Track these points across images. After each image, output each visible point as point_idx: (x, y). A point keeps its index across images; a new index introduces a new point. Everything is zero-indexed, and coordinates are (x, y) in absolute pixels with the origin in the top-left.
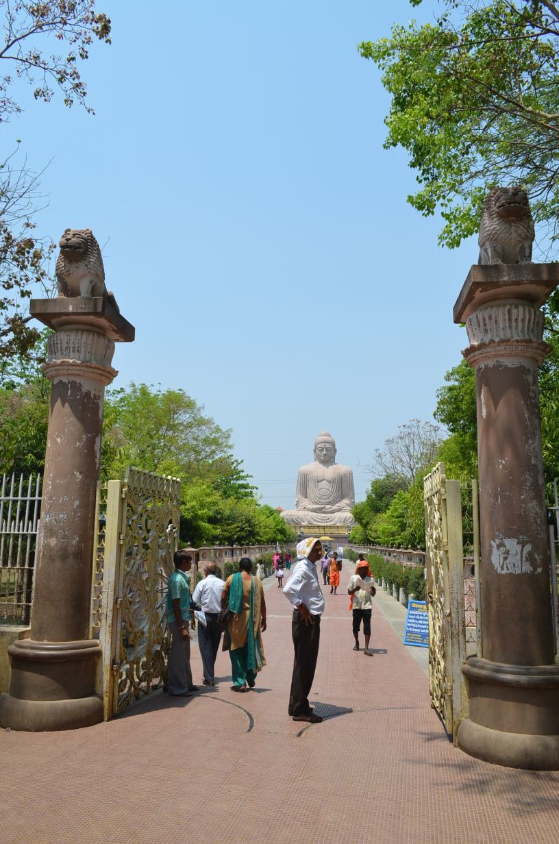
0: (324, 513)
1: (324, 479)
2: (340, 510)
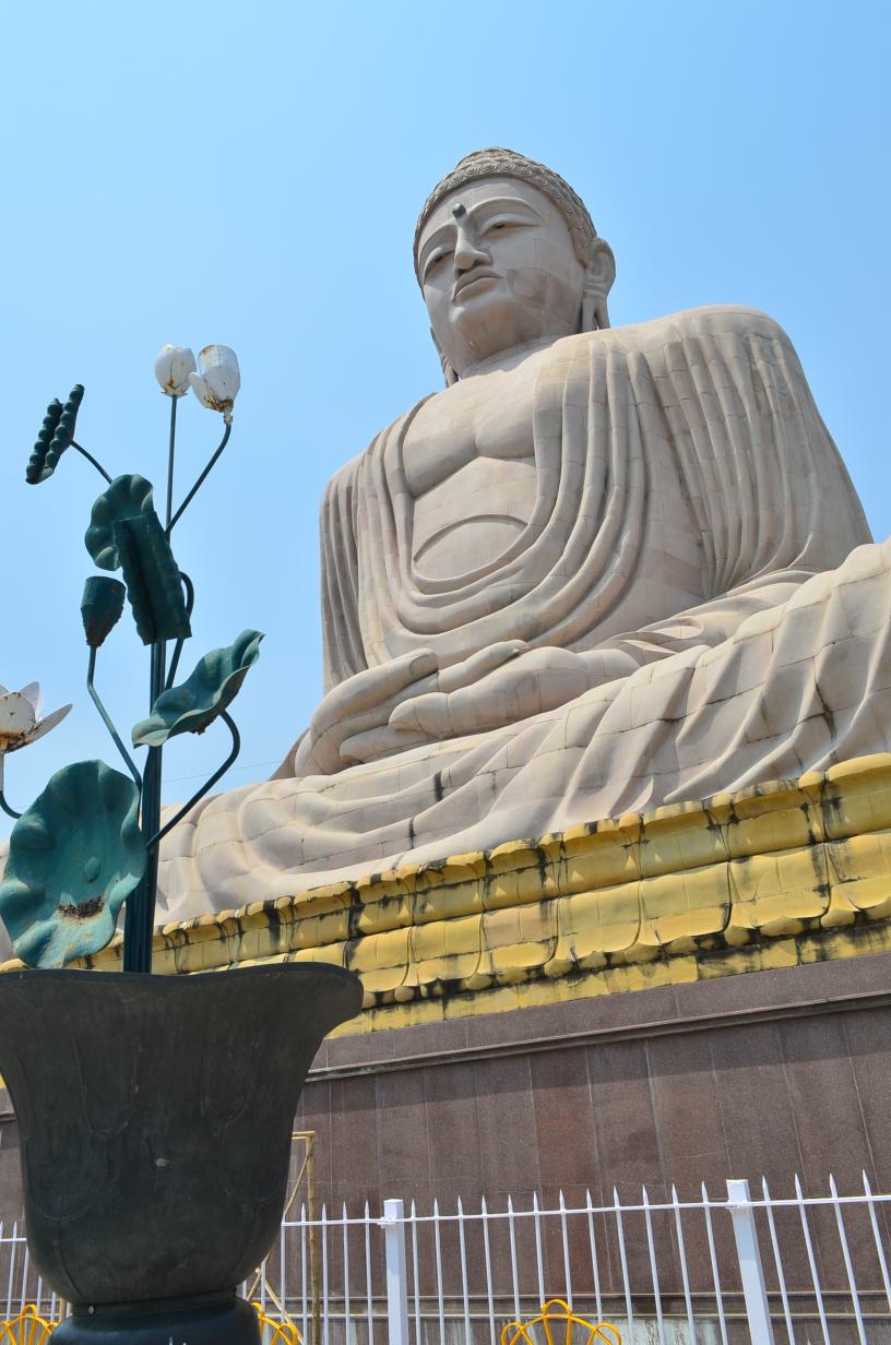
1: (472, 451)
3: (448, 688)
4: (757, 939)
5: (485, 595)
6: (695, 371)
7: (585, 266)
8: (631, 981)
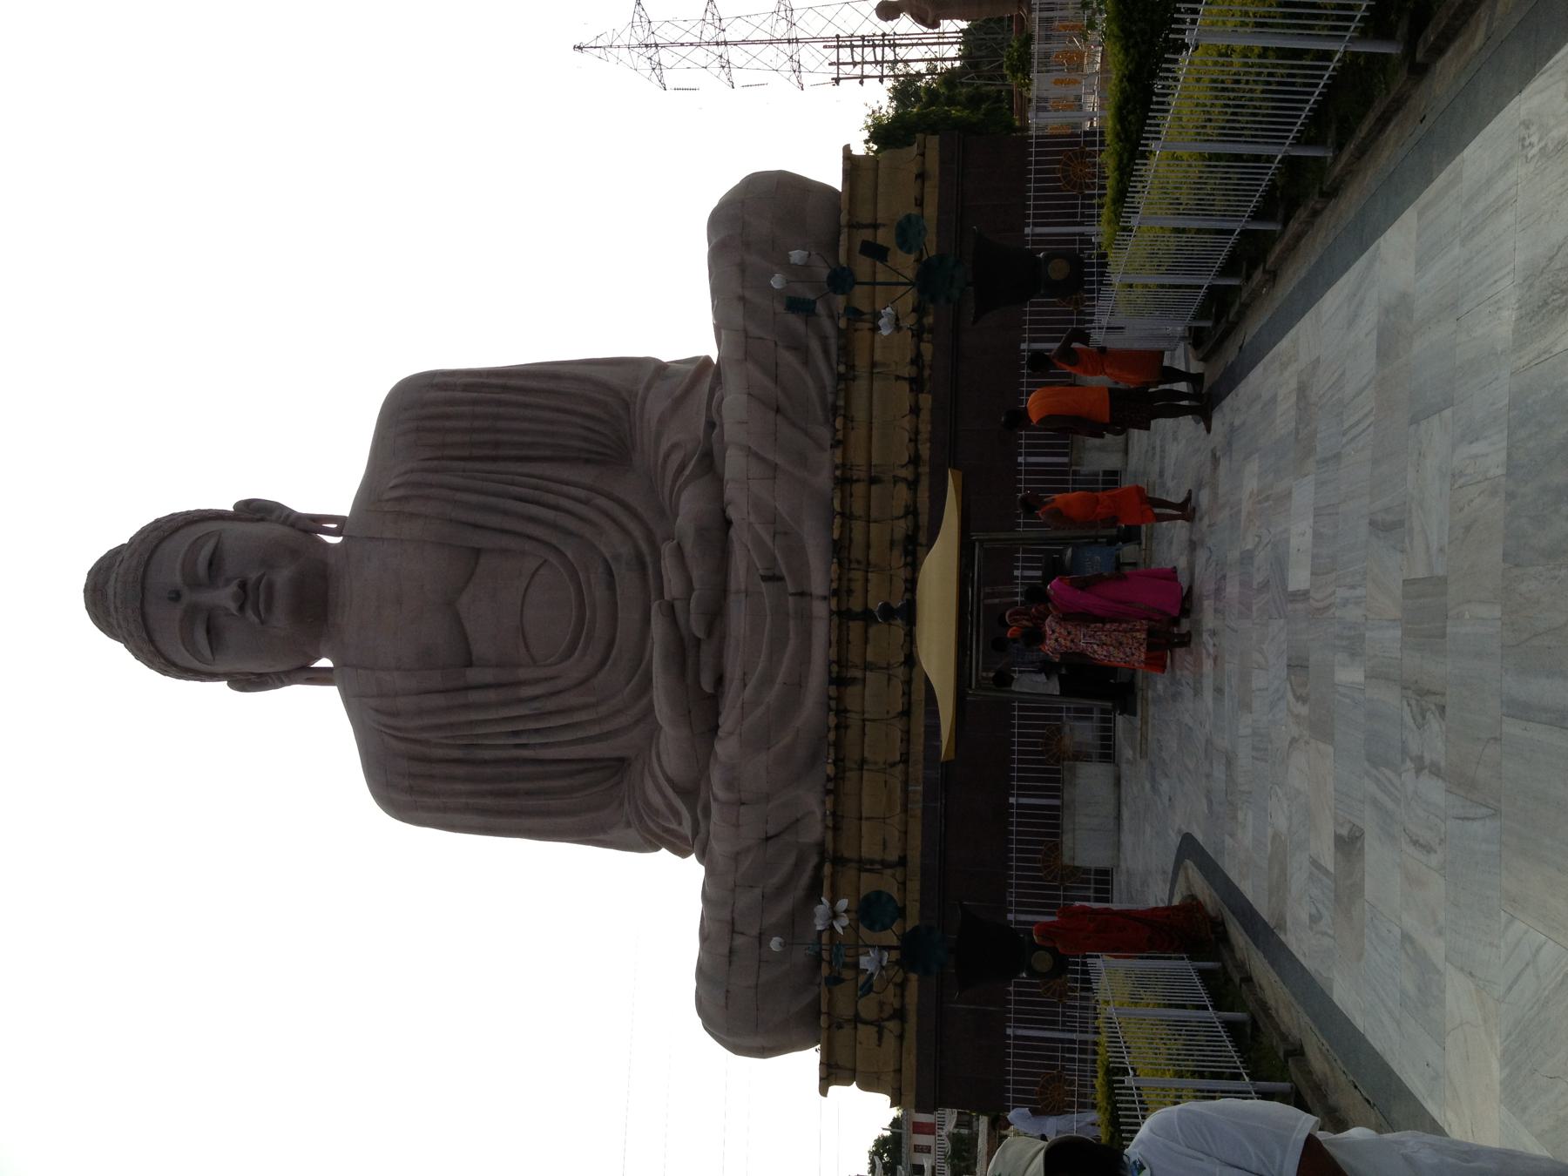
0: (716, 614)
2: (709, 462)
3: (690, 587)
4: (917, 360)
6: (448, 424)
7: (262, 520)
8: (925, 428)
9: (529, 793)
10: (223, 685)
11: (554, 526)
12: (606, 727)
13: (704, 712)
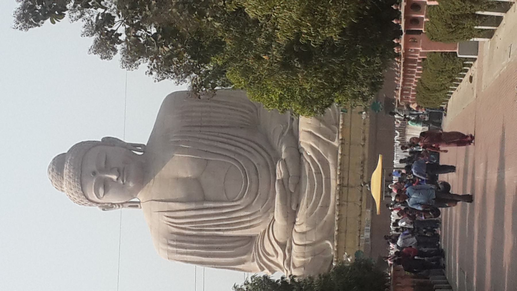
5: (254, 177)
7: (114, 146)
8: (367, 130)
9: (218, 248)
10: (97, 208)
11: (235, 153)
12: (252, 224)
13: (291, 217)
